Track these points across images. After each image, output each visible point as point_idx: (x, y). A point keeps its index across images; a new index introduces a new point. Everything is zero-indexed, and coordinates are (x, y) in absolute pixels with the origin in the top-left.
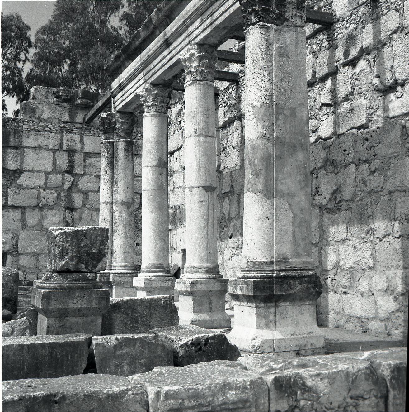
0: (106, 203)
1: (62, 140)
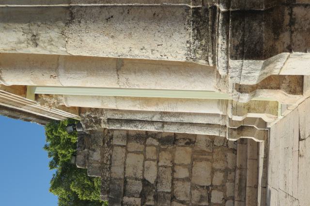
0: (163, 126)
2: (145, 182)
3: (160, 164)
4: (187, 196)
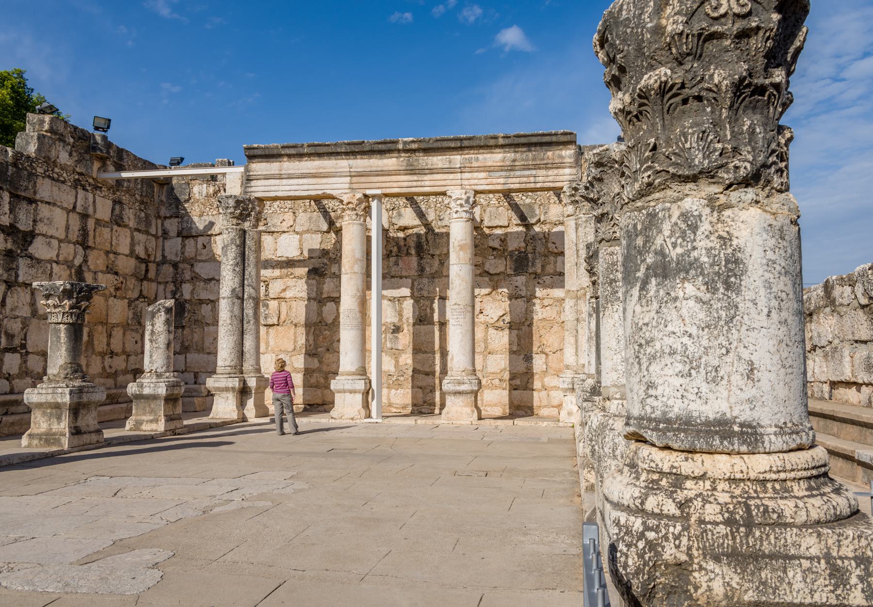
1: (76, 197)
2: (29, 237)
3: (54, 265)
4: (12, 310)
